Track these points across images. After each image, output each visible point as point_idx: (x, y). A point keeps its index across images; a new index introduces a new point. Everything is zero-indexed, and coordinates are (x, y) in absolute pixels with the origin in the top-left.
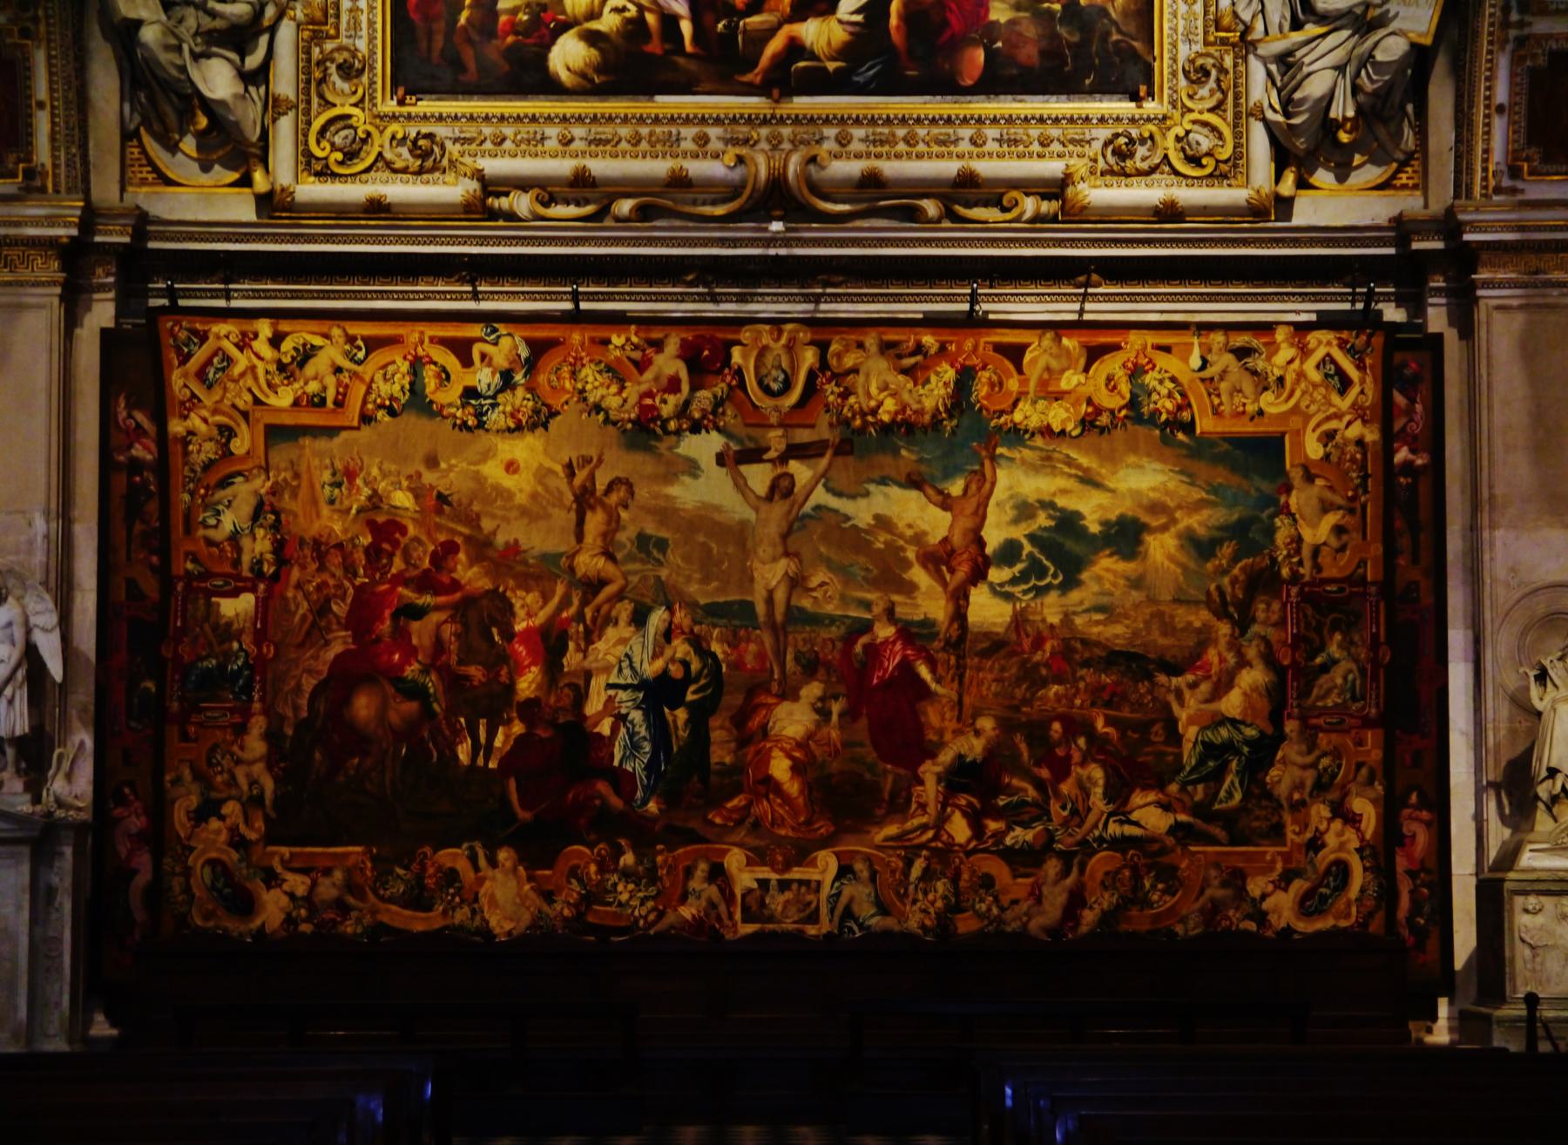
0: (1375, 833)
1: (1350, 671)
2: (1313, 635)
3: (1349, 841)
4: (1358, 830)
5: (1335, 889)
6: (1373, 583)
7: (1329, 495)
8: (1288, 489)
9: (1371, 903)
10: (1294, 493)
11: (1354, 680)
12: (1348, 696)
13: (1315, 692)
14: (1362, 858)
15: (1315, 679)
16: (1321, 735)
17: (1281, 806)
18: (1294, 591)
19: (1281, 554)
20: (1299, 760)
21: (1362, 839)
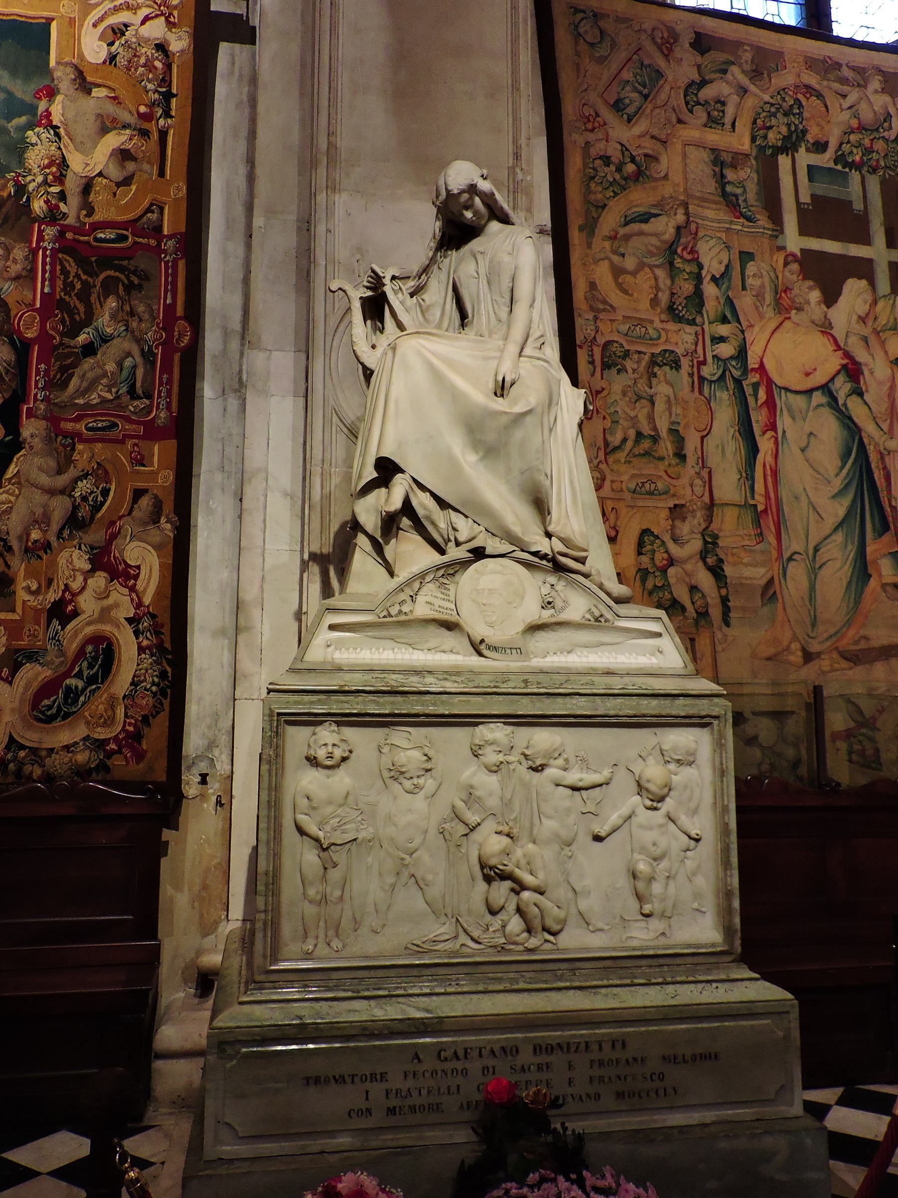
0: (158, 593)
1: (129, 354)
2: (75, 302)
3: (117, 605)
4: (132, 589)
5: (91, 680)
6: (170, 237)
7: (110, 108)
8: (51, 93)
9: (147, 701)
10: (59, 98)
11: (135, 367)
12: (124, 390)
13: (74, 383)
14: (137, 633)
15: (74, 365)
16: (80, 447)
17: (10, 549)
18: (50, 232)
19: (33, 183)
20: (44, 480)
21: (139, 605)
